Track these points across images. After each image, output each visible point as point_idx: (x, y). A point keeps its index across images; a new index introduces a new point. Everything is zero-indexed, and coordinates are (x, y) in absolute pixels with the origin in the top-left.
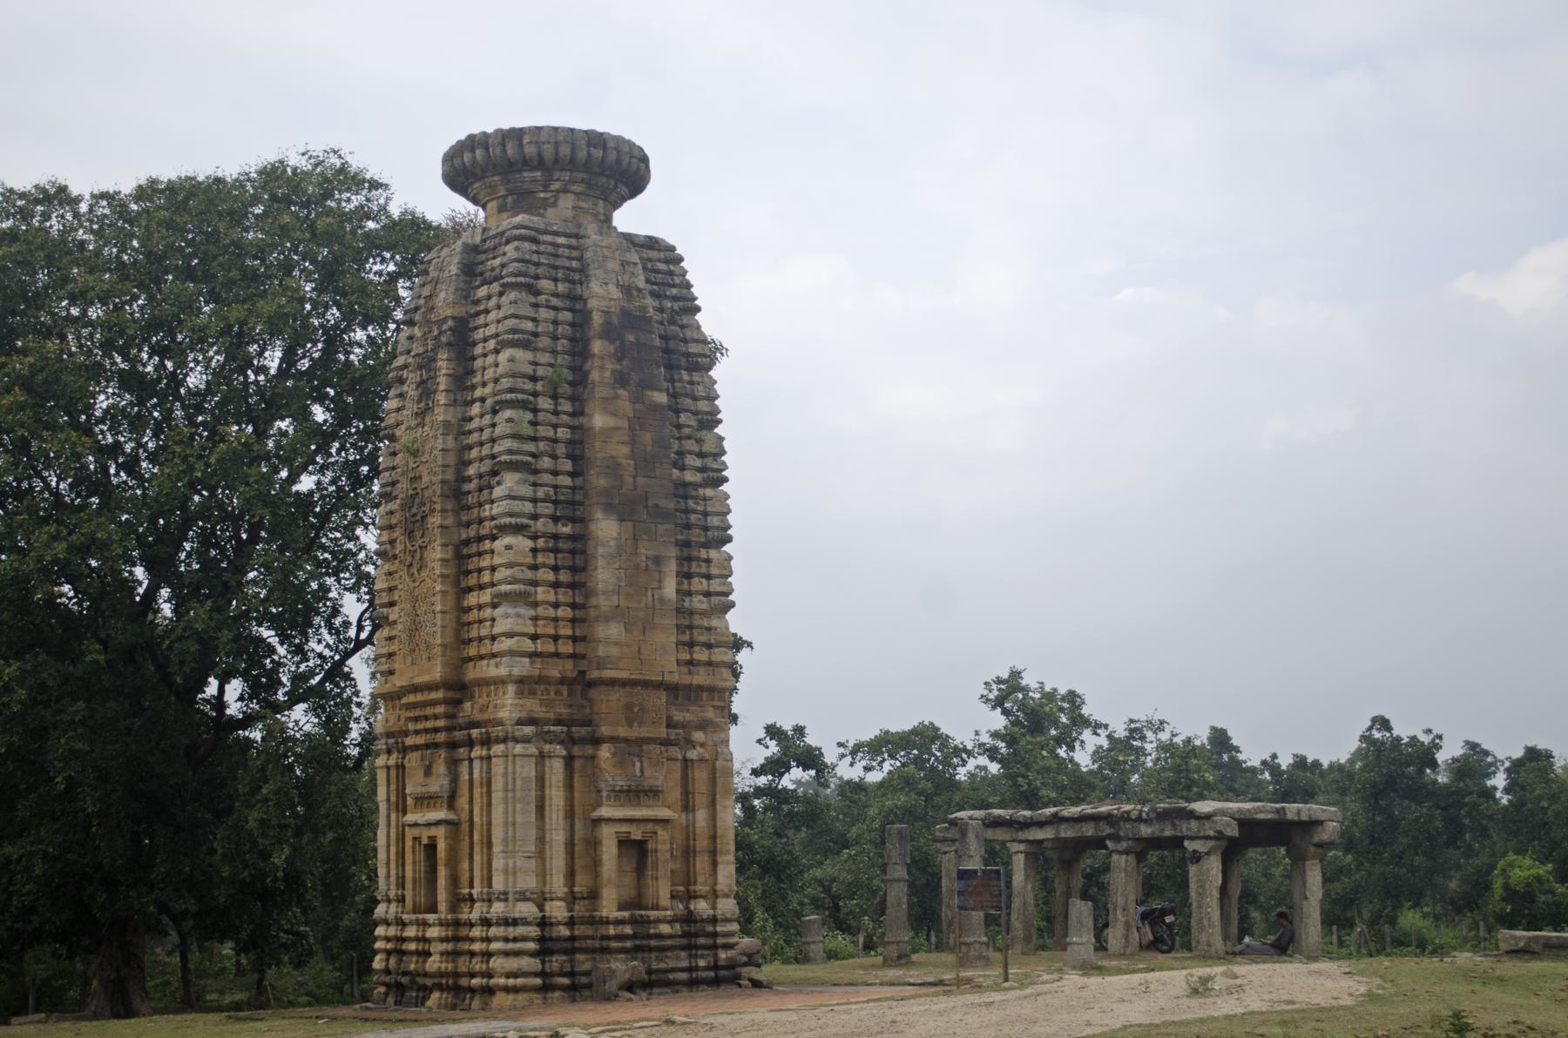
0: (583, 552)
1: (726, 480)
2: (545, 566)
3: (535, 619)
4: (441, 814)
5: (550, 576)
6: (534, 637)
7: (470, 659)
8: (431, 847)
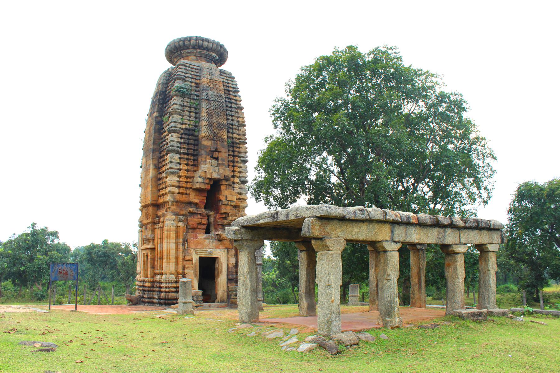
0: (197, 160)
1: (246, 143)
2: (183, 164)
3: (179, 182)
4: (150, 246)
5: (186, 167)
6: (179, 187)
7: (160, 196)
8: (147, 256)
